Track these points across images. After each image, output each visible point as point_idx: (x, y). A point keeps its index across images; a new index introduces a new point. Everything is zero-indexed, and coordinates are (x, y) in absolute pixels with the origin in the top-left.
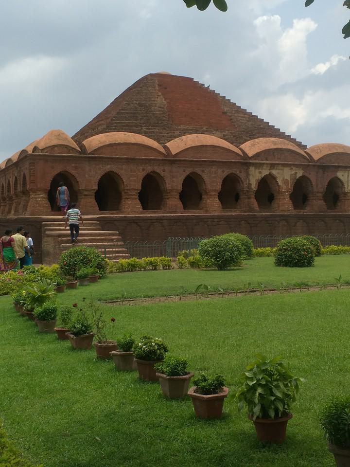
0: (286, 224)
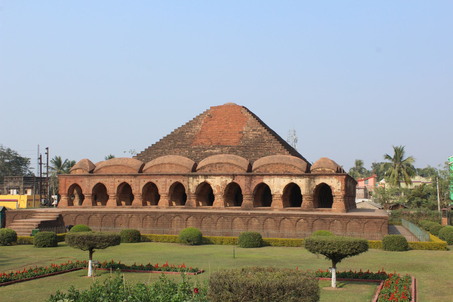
0: (179, 218)
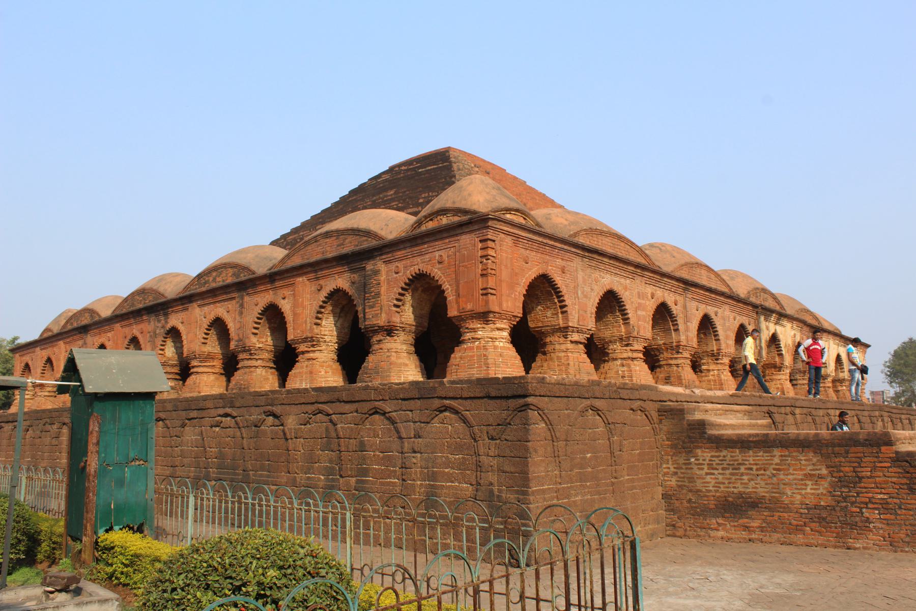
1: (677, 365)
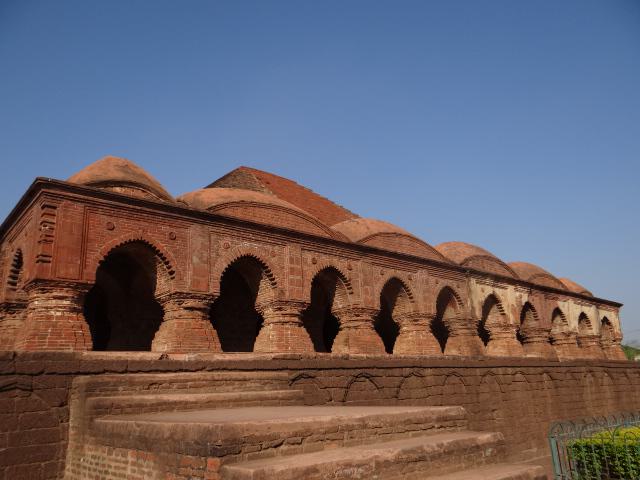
0: (592, 379)
1: (356, 328)
